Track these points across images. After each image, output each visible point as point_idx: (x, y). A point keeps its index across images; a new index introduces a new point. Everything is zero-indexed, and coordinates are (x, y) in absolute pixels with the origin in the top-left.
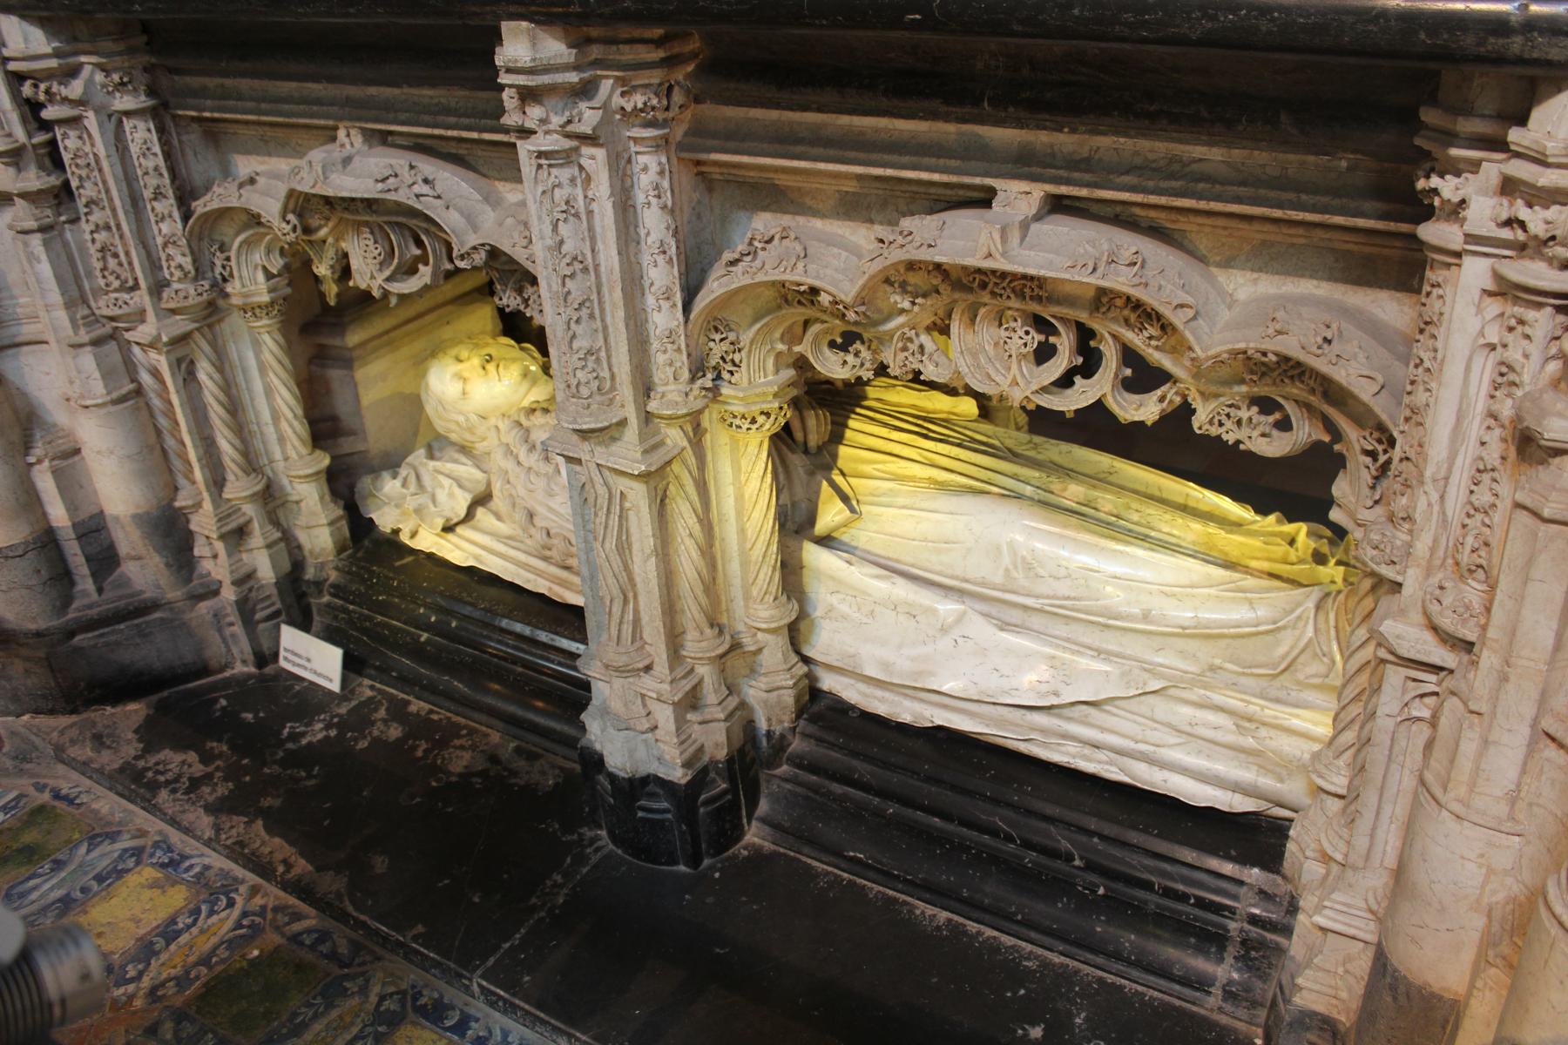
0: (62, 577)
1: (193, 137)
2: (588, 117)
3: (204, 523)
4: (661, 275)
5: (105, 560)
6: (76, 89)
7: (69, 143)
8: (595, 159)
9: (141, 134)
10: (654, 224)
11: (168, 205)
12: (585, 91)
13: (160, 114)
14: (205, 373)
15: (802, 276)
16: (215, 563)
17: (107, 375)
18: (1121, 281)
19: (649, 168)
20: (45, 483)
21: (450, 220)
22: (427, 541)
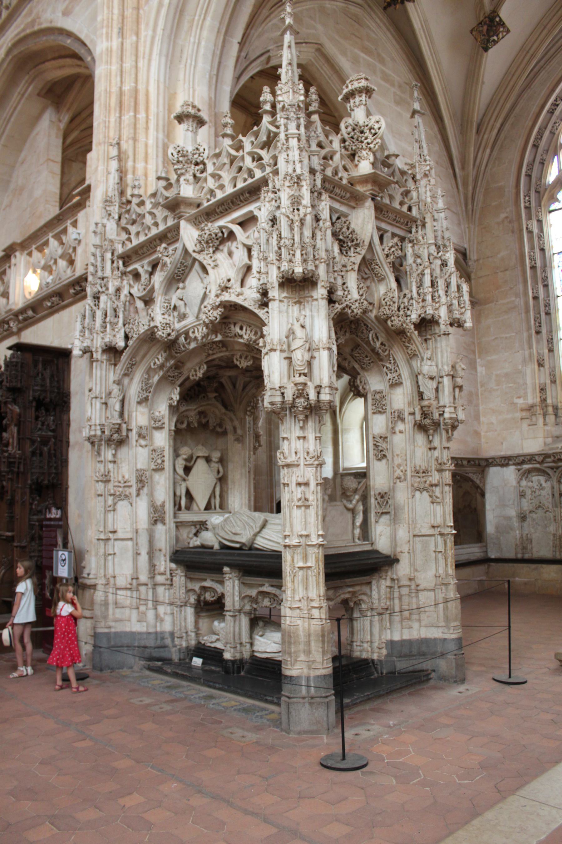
0: (156, 639)
1: (189, 580)
2: (231, 576)
3: (176, 635)
4: (237, 594)
5: (163, 639)
6: (176, 572)
7: (174, 578)
8: (231, 581)
9: (183, 578)
10: (237, 588)
11: (184, 588)
12: (230, 573)
13: (186, 576)
14: (183, 612)
15: (250, 594)
16: (177, 641)
17: (171, 610)
18: (274, 592)
19: (237, 582)
20: (158, 624)
21: (218, 590)
22: (209, 644)
